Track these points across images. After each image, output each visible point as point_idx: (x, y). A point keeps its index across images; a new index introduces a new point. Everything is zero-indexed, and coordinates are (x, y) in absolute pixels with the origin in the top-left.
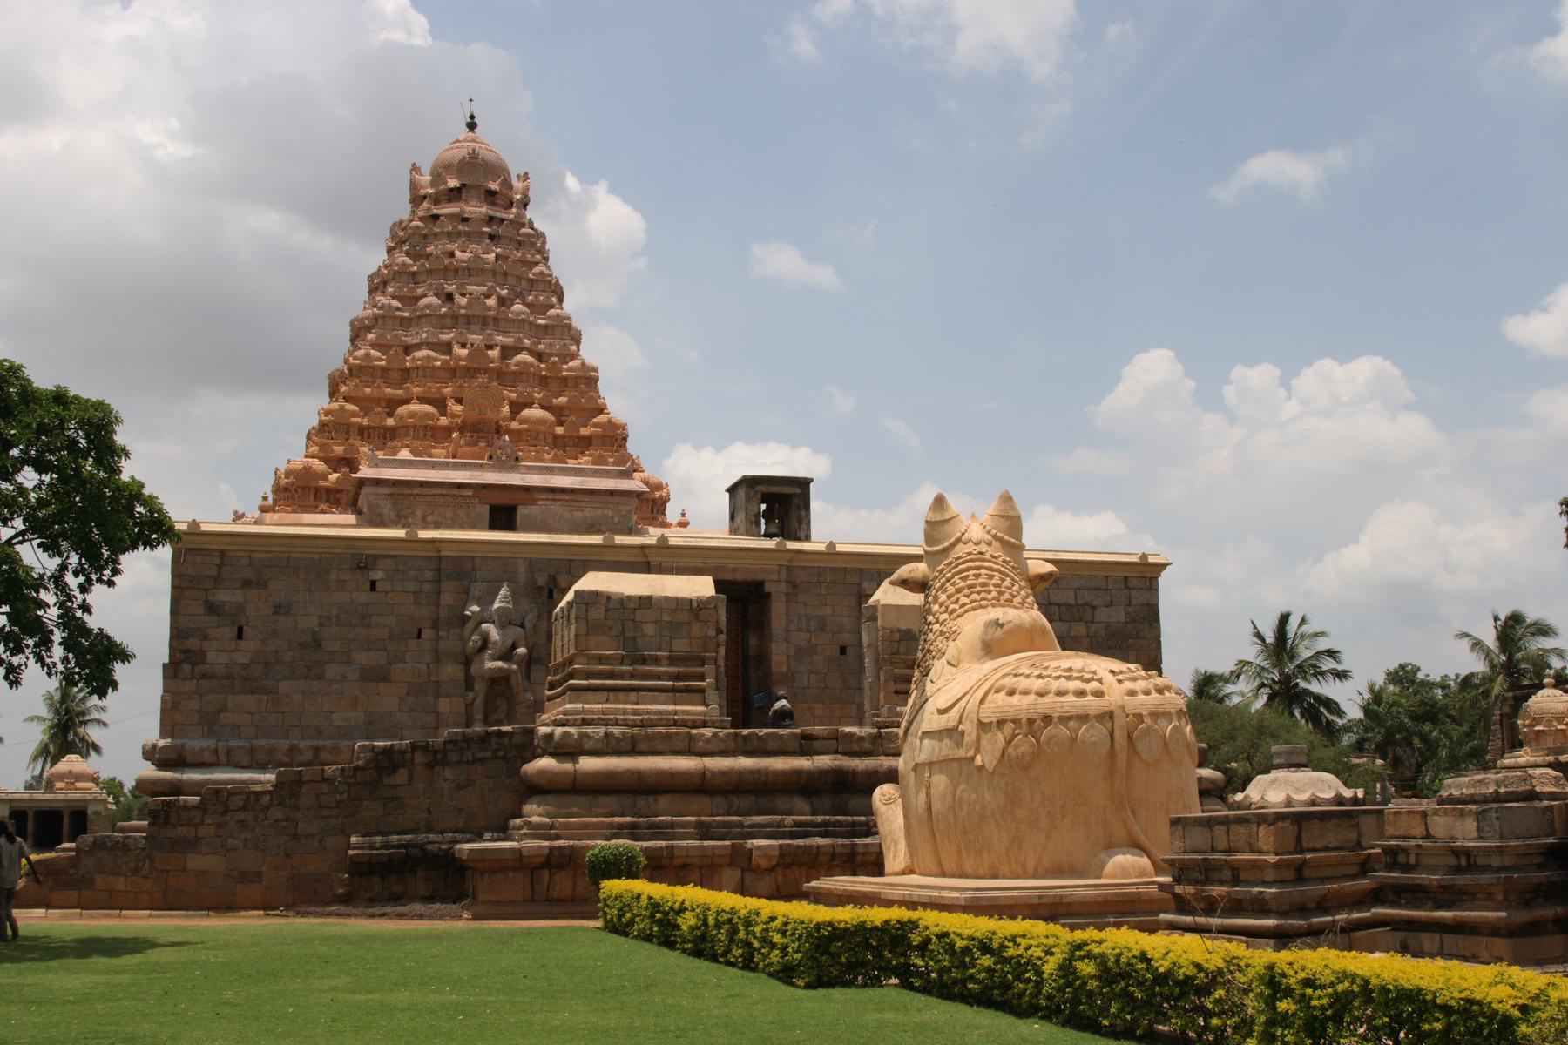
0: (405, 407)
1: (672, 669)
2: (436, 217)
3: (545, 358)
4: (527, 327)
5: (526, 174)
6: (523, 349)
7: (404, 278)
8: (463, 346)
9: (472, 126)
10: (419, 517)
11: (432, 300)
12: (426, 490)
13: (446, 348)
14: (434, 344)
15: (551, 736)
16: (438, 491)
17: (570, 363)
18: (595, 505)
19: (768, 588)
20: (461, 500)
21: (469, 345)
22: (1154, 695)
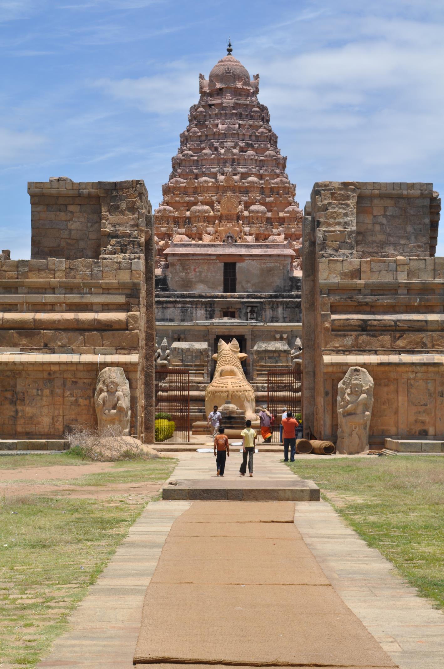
0: (195, 207)
1: (195, 368)
2: (210, 106)
3: (263, 177)
4: (254, 162)
5: (258, 75)
6: (252, 174)
7: (195, 139)
8: (223, 174)
9: (230, 51)
10: (193, 270)
11: (208, 151)
12: (195, 257)
13: (214, 176)
14: (208, 174)
15: (161, 386)
16: (200, 258)
17: (275, 180)
18: (271, 261)
19: (246, 337)
20: (211, 261)
21: (225, 174)
22: (239, 387)
